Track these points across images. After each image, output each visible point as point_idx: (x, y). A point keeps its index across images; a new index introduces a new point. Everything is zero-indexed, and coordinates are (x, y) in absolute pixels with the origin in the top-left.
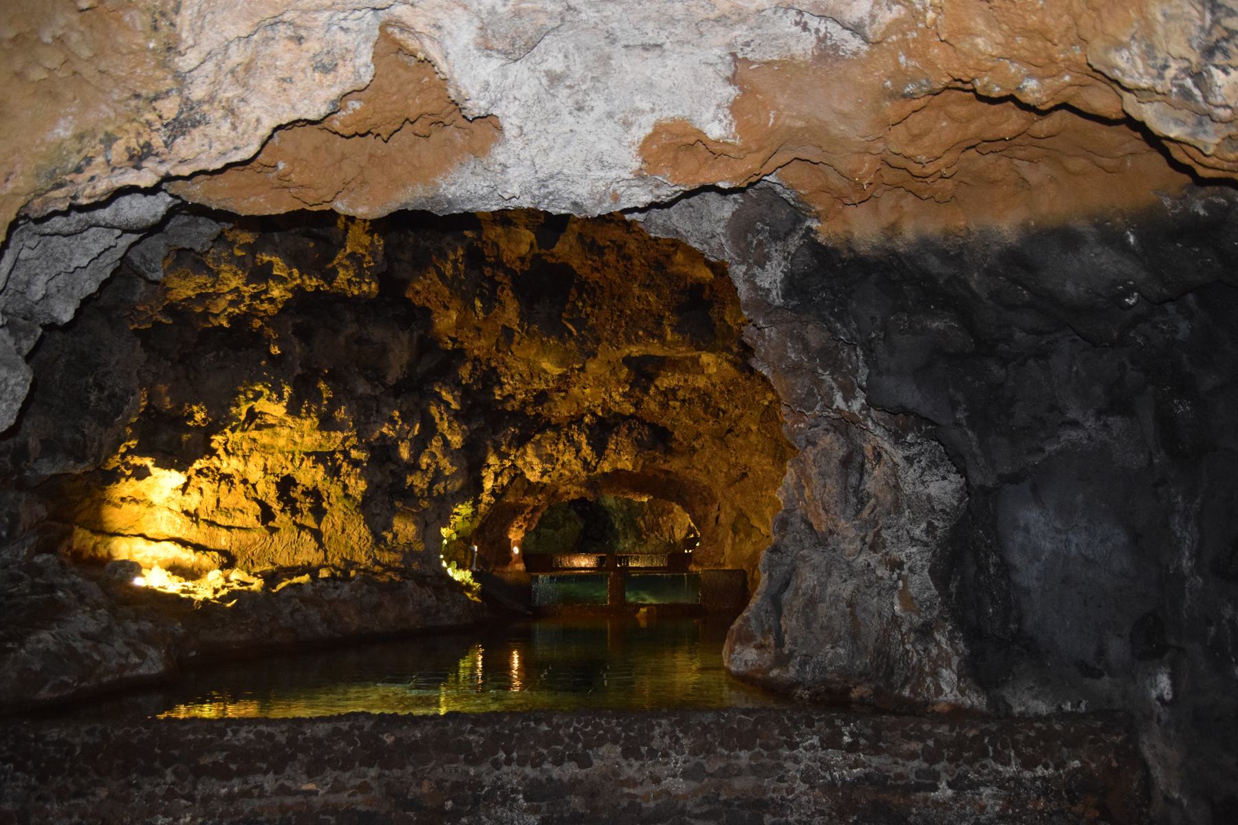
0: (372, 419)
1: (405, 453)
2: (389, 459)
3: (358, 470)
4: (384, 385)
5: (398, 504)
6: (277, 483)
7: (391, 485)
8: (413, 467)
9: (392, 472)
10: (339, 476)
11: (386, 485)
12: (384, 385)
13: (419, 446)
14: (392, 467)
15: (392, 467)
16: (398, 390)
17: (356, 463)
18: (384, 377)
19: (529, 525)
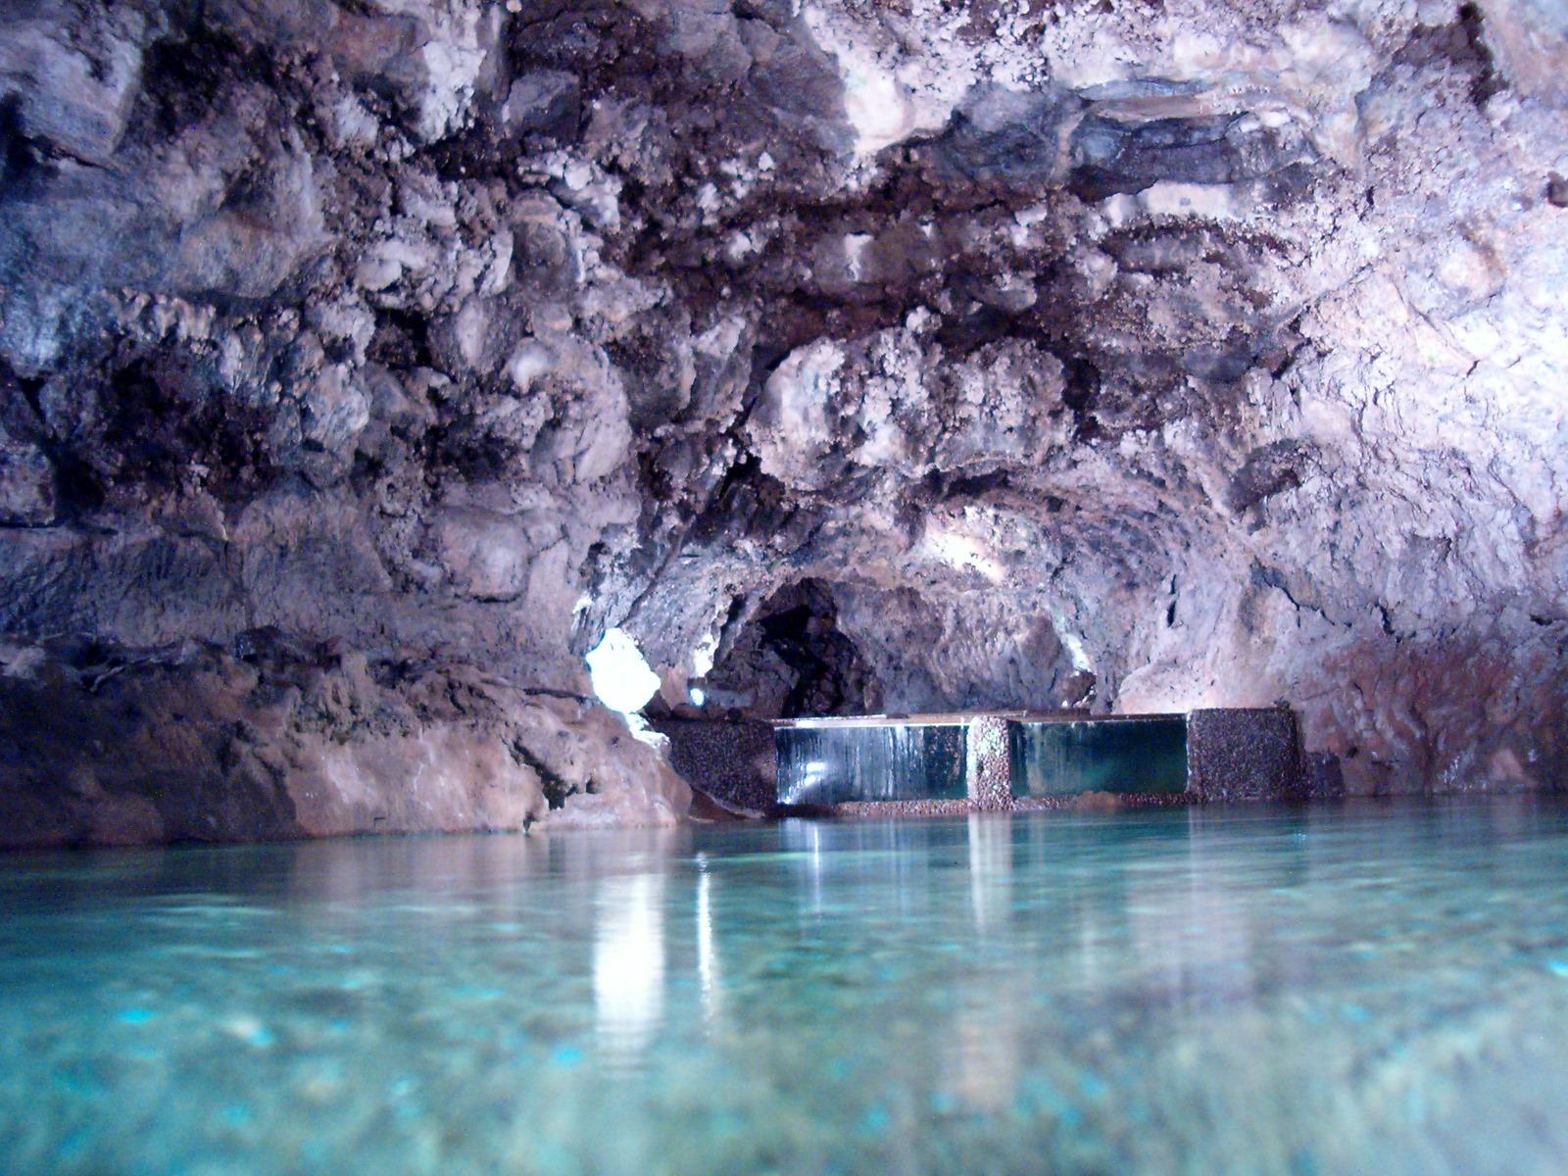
0: (379, 227)
1: (470, 336)
2: (426, 359)
3: (342, 369)
4: (413, 138)
5: (456, 493)
6: (101, 389)
7: (435, 434)
8: (498, 385)
9: (434, 395)
10: (287, 384)
11: (418, 431)
12: (413, 138)
13: (513, 326)
14: (438, 381)
15: (438, 381)
16: (452, 158)
17: (337, 351)
18: (414, 113)
19: (723, 643)
